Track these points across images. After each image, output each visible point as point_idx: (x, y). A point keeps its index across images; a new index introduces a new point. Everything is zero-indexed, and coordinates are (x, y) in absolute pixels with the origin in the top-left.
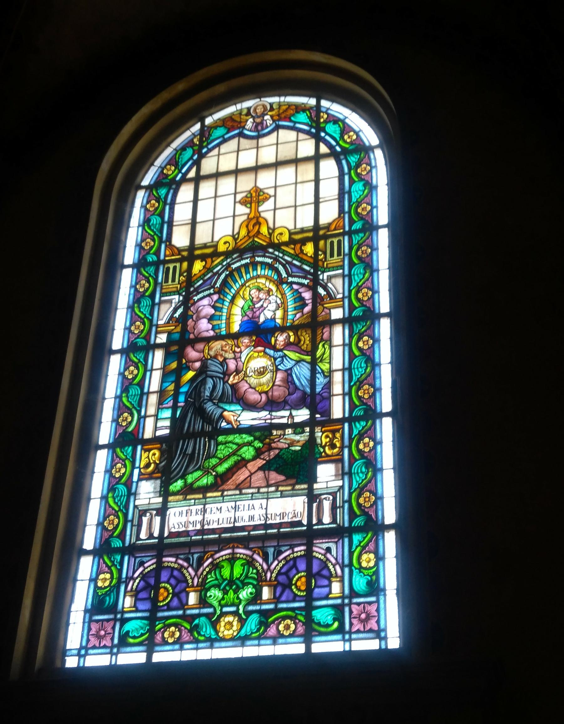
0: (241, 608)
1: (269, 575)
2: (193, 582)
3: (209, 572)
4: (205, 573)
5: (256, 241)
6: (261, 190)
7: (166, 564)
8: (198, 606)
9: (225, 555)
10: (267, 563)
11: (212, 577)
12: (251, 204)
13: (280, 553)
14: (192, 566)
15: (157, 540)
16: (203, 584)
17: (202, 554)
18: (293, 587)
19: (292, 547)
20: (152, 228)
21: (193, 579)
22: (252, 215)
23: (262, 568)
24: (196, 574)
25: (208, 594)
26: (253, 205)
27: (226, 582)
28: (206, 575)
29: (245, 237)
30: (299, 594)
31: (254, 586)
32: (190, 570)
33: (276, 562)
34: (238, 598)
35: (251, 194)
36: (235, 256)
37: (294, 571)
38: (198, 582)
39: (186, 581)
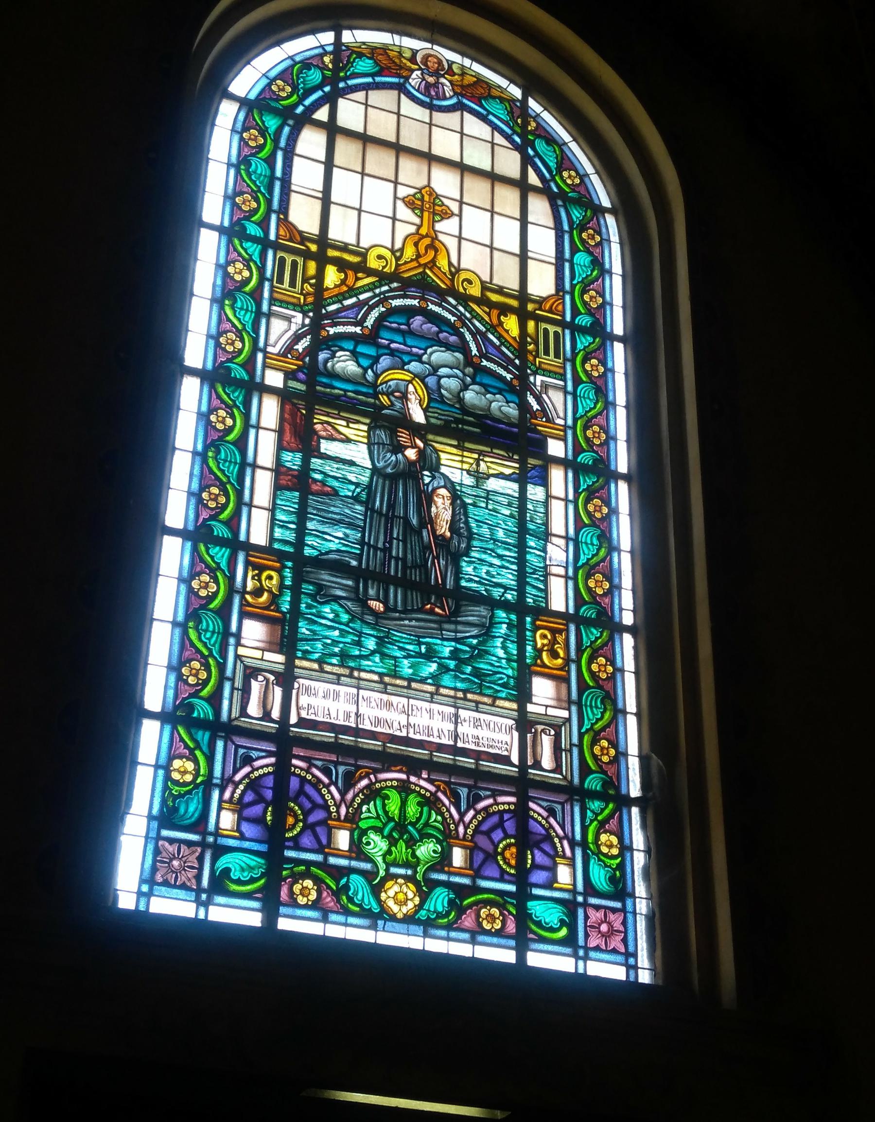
2: (338, 812)
3: (364, 802)
6: (437, 196)
8: (347, 854)
9: (391, 780)
10: (458, 809)
11: (369, 811)
12: (422, 211)
14: (336, 784)
20: (253, 177)
21: (338, 807)
22: (423, 231)
23: (451, 816)
24: (343, 799)
27: (392, 824)
28: (360, 805)
29: (412, 260)
32: (333, 789)
33: (471, 813)
36: (395, 285)
38: (348, 812)
39: (326, 807)
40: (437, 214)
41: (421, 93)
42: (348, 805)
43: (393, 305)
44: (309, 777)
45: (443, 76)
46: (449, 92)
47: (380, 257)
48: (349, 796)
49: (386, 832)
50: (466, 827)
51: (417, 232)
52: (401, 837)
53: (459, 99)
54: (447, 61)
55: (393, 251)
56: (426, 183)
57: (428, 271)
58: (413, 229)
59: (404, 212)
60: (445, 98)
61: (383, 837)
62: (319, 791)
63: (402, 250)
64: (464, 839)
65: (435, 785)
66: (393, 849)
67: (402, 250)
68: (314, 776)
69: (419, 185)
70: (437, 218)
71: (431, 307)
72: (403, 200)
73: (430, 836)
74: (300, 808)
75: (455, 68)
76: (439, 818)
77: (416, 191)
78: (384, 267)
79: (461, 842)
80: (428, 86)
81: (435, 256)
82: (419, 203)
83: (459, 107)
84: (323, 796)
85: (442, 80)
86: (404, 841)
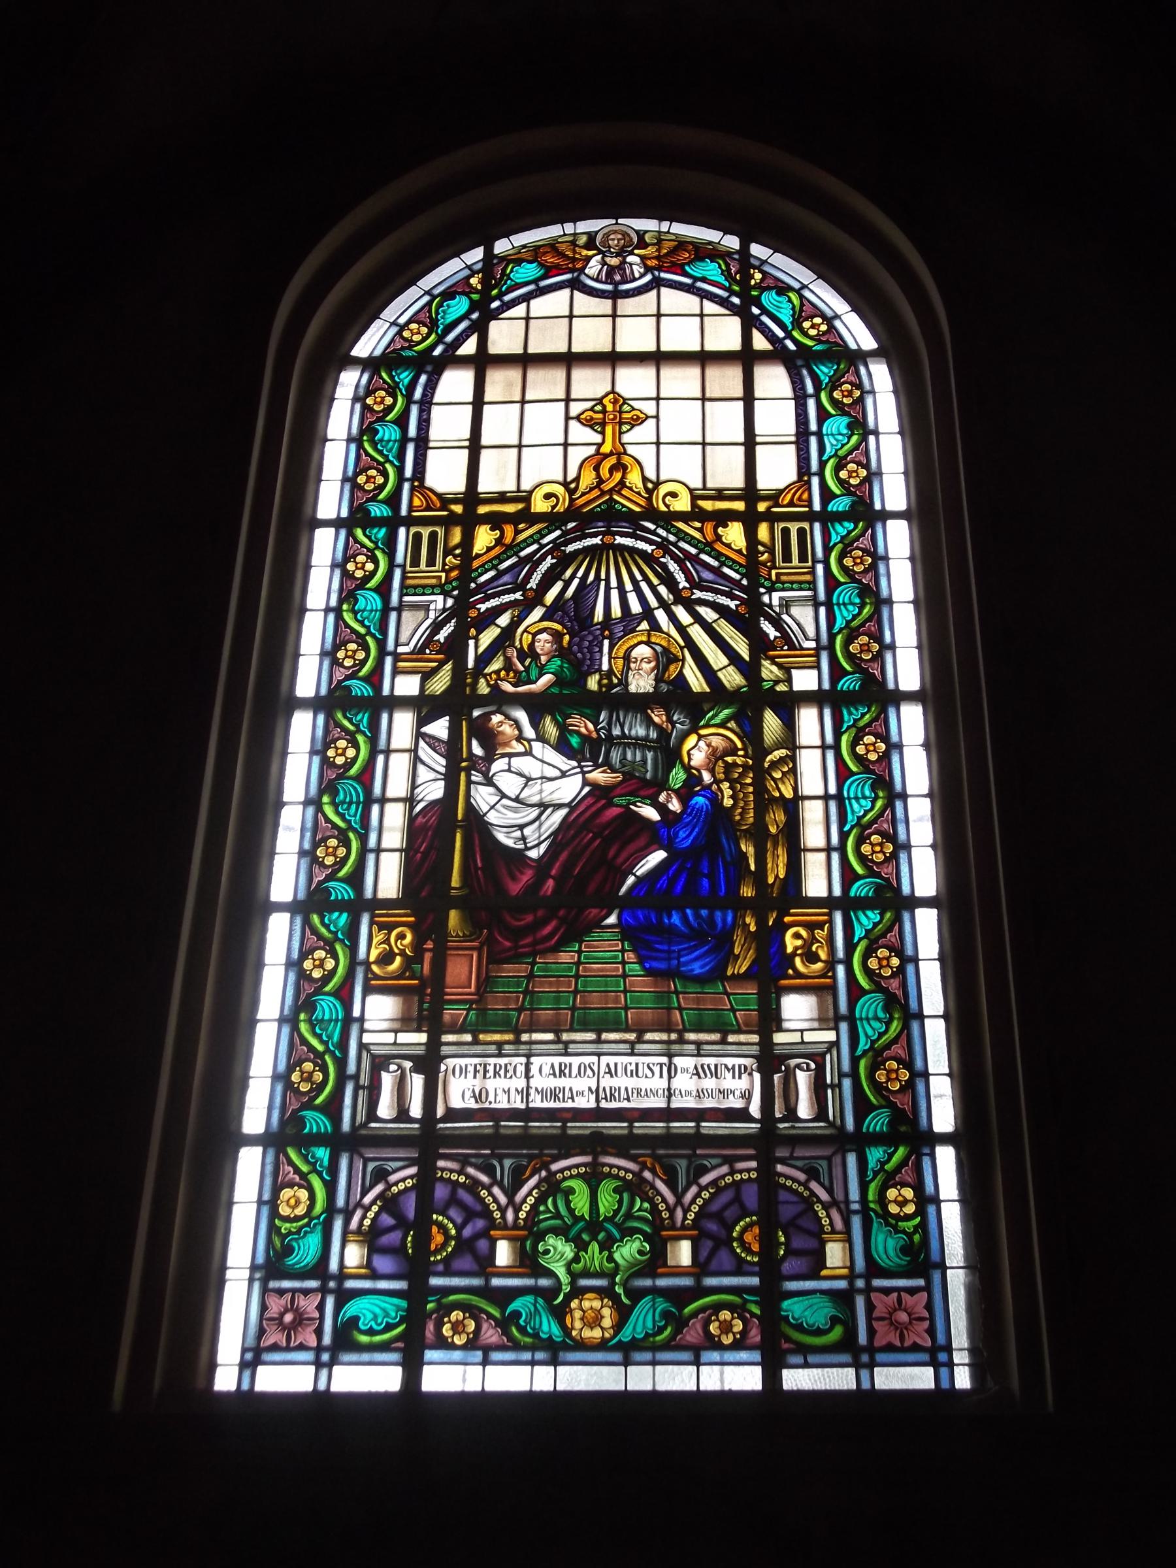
1: (679, 1213)
5: (617, 502)
6: (625, 401)
12: (603, 424)
22: (606, 448)
26: (609, 429)
27: (581, 1224)
29: (592, 489)
35: (604, 407)
40: (626, 423)
41: (601, 282)
46: (637, 270)
47: (548, 496)
51: (598, 452)
54: (637, 232)
55: (565, 484)
56: (609, 389)
58: (592, 450)
59: (579, 433)
63: (577, 479)
67: (577, 479)
69: (599, 396)
70: (625, 428)
71: (619, 540)
72: (578, 418)
77: (593, 403)
78: (553, 507)
80: (611, 270)
82: (600, 416)
85: (630, 259)
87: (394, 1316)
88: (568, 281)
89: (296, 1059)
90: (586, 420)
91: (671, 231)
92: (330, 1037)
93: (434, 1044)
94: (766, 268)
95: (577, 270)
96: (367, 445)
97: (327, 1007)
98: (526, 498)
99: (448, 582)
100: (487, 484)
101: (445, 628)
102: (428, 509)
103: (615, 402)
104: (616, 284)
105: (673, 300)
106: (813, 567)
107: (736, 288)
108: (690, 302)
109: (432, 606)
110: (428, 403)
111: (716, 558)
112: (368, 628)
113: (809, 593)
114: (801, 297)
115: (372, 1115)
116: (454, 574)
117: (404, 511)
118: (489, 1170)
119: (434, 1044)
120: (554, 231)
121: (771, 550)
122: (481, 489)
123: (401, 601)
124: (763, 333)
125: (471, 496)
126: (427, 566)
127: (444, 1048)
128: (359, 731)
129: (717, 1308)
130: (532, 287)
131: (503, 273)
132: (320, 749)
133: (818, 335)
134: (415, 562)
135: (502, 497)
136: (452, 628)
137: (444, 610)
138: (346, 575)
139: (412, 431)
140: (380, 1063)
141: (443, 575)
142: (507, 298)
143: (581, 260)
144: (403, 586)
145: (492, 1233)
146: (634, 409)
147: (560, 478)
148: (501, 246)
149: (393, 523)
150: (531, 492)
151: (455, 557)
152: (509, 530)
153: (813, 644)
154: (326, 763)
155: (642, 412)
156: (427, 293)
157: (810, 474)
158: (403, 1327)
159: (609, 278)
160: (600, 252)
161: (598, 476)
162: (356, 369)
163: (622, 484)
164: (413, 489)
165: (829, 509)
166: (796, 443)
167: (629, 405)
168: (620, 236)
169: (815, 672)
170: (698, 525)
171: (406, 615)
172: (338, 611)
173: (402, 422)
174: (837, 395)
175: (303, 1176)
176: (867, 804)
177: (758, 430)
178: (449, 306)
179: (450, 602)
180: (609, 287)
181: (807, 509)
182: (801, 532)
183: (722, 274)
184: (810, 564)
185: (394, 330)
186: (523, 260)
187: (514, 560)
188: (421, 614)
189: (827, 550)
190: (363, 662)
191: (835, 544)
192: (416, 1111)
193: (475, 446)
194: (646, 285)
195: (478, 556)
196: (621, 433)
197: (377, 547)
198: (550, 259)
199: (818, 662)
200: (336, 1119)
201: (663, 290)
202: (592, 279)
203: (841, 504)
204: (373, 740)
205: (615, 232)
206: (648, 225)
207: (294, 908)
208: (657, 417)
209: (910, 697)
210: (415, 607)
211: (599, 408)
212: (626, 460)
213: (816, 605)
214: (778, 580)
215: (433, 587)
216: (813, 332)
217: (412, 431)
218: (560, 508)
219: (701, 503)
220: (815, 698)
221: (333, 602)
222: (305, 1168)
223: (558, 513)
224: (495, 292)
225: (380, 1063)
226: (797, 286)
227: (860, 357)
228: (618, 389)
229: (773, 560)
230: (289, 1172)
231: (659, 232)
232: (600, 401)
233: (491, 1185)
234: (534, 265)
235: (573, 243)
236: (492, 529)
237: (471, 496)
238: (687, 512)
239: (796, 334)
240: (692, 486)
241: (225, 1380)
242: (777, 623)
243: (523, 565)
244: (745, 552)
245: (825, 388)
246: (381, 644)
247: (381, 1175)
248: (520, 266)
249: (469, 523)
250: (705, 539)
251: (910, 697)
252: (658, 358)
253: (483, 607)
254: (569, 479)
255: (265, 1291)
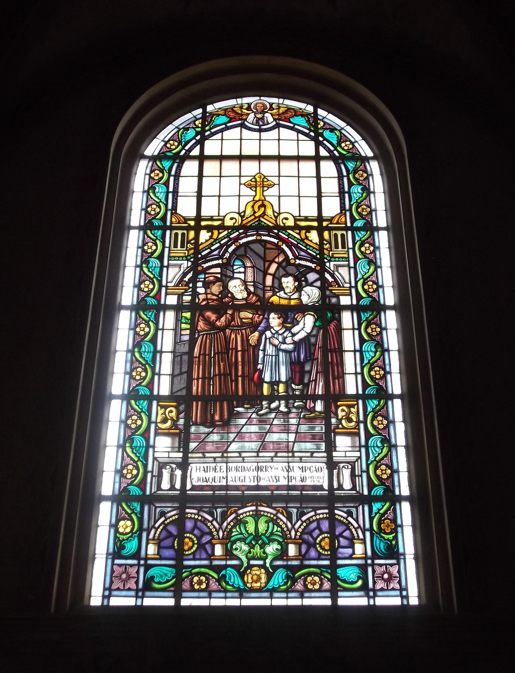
0: (268, 561)
1: (293, 533)
2: (218, 534)
3: (234, 526)
4: (229, 527)
5: (262, 222)
6: (265, 177)
7: (189, 516)
10: (291, 522)
12: (256, 187)
13: (303, 514)
14: (216, 520)
15: (179, 492)
16: (229, 537)
17: (226, 509)
18: (317, 546)
19: (315, 509)
22: (257, 198)
23: (287, 526)
25: (234, 547)
26: (258, 189)
28: (231, 529)
29: (251, 216)
30: (323, 552)
31: (279, 543)
34: (264, 552)
35: (256, 179)
37: (317, 531)
38: (223, 534)
39: (211, 533)
40: (265, 187)
41: (254, 125)
42: (224, 530)
43: (241, 243)
44: (200, 518)
45: (267, 112)
46: (270, 119)
47: (232, 219)
48: (225, 524)
49: (247, 541)
50: (296, 532)
51: (254, 200)
52: (257, 543)
53: (276, 122)
54: (269, 103)
55: (239, 213)
56: (258, 172)
57: (262, 219)
58: (251, 198)
60: (268, 124)
61: (245, 544)
62: (206, 525)
63: (244, 212)
64: (295, 538)
65: (276, 510)
66: (252, 550)
67: (244, 212)
68: (202, 517)
69: (254, 175)
70: (265, 188)
72: (244, 184)
73: (274, 540)
74: (195, 535)
75: (274, 106)
76: (279, 529)
78: (234, 224)
79: (294, 541)
80: (258, 119)
81: (265, 210)
82: (254, 183)
83: (278, 126)
84: (208, 527)
85: (266, 115)
86: (258, 544)
87: (170, 575)
88: (239, 124)
89: (125, 464)
90: (248, 185)
91: (284, 103)
92: (140, 453)
93: (185, 458)
94: (325, 120)
95: (243, 119)
96: (151, 194)
97: (139, 441)
98: (223, 220)
99: (188, 255)
100: (204, 213)
101: (188, 275)
102: (179, 223)
103: (260, 177)
104: (260, 126)
105: (285, 133)
106: (348, 251)
107: (313, 129)
108: (293, 134)
109: (182, 266)
110: (177, 176)
111: (305, 247)
112: (154, 275)
113: (347, 263)
114: (341, 133)
115: (159, 488)
116: (192, 251)
117: (168, 224)
118: (211, 514)
119: (185, 458)
120: (231, 102)
121: (330, 243)
122: (203, 214)
123: (168, 263)
124: (324, 148)
125: (198, 218)
126: (181, 248)
127: (190, 459)
128: (150, 320)
129: (310, 574)
130: (224, 126)
131: (211, 120)
132: (134, 328)
133: (348, 149)
134: (176, 246)
135: (211, 219)
136: (191, 275)
137: (188, 267)
138: (144, 251)
139: (171, 189)
140: (162, 466)
141: (187, 252)
142: (213, 131)
143: (245, 115)
144: (169, 257)
145: (213, 541)
146: (268, 180)
147: (237, 211)
148: (210, 108)
149: (164, 228)
150: (225, 217)
151: (192, 244)
152: (216, 232)
153: (348, 285)
154: (136, 333)
155: (272, 182)
156: (177, 127)
157: (346, 211)
158: (174, 580)
159: (257, 123)
160: (253, 112)
161: (254, 210)
162: (146, 160)
163: (264, 214)
164: (172, 214)
165: (354, 225)
166: (340, 196)
167: (266, 179)
168: (262, 105)
169: (349, 297)
170: (298, 231)
171: (170, 269)
172: (141, 267)
173: (167, 184)
174: (357, 176)
175: (130, 515)
176: (372, 354)
177: (323, 190)
178: (186, 133)
179: (190, 264)
180: (258, 127)
181: (344, 225)
182: (342, 236)
183: (306, 122)
184: (346, 250)
185: (163, 143)
186: (220, 115)
187: (218, 245)
188: (177, 269)
189: (354, 244)
190: (152, 290)
191: (358, 241)
192: (178, 486)
193: (199, 196)
194: (273, 126)
195: (202, 244)
196: (263, 191)
197: (157, 239)
198: (232, 115)
199: (351, 293)
200: (144, 490)
201: (281, 128)
202: (250, 123)
203: (359, 223)
204: (157, 324)
205: (260, 103)
206: (275, 100)
207: (123, 397)
208: (279, 184)
209: (390, 308)
210: (175, 265)
211: (254, 180)
212: (266, 203)
213: (350, 268)
214: (332, 257)
215: (182, 257)
216: (346, 148)
217: (171, 189)
218: (236, 224)
219: (298, 223)
220: (350, 308)
221: (139, 263)
222: (129, 511)
223: (236, 226)
224: (207, 128)
225: (162, 466)
226: (339, 129)
227: (366, 159)
228: (261, 172)
229: (331, 248)
230: (123, 513)
231: (279, 103)
232: (254, 177)
233: (212, 521)
234: (225, 116)
235: (241, 107)
236: (208, 232)
237: (198, 218)
238: (293, 226)
239: (338, 148)
240: (295, 215)
241: (96, 601)
242: (332, 276)
243: (221, 249)
244: (318, 244)
245: (351, 173)
246: (160, 282)
247: (163, 514)
248: (218, 117)
249: (198, 229)
250: (301, 237)
251: (390, 308)
252: (279, 158)
253: (205, 266)
254: (241, 212)
255: (113, 564)
